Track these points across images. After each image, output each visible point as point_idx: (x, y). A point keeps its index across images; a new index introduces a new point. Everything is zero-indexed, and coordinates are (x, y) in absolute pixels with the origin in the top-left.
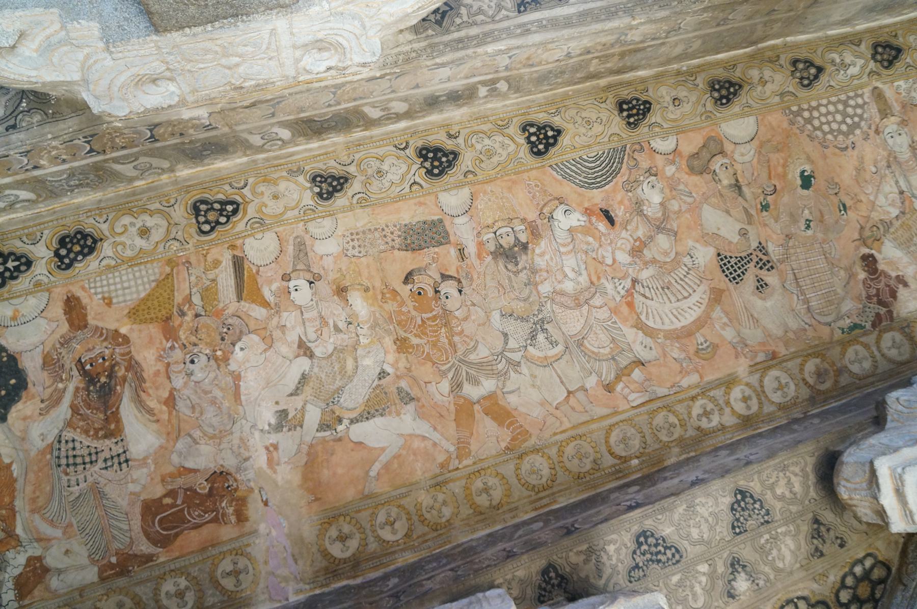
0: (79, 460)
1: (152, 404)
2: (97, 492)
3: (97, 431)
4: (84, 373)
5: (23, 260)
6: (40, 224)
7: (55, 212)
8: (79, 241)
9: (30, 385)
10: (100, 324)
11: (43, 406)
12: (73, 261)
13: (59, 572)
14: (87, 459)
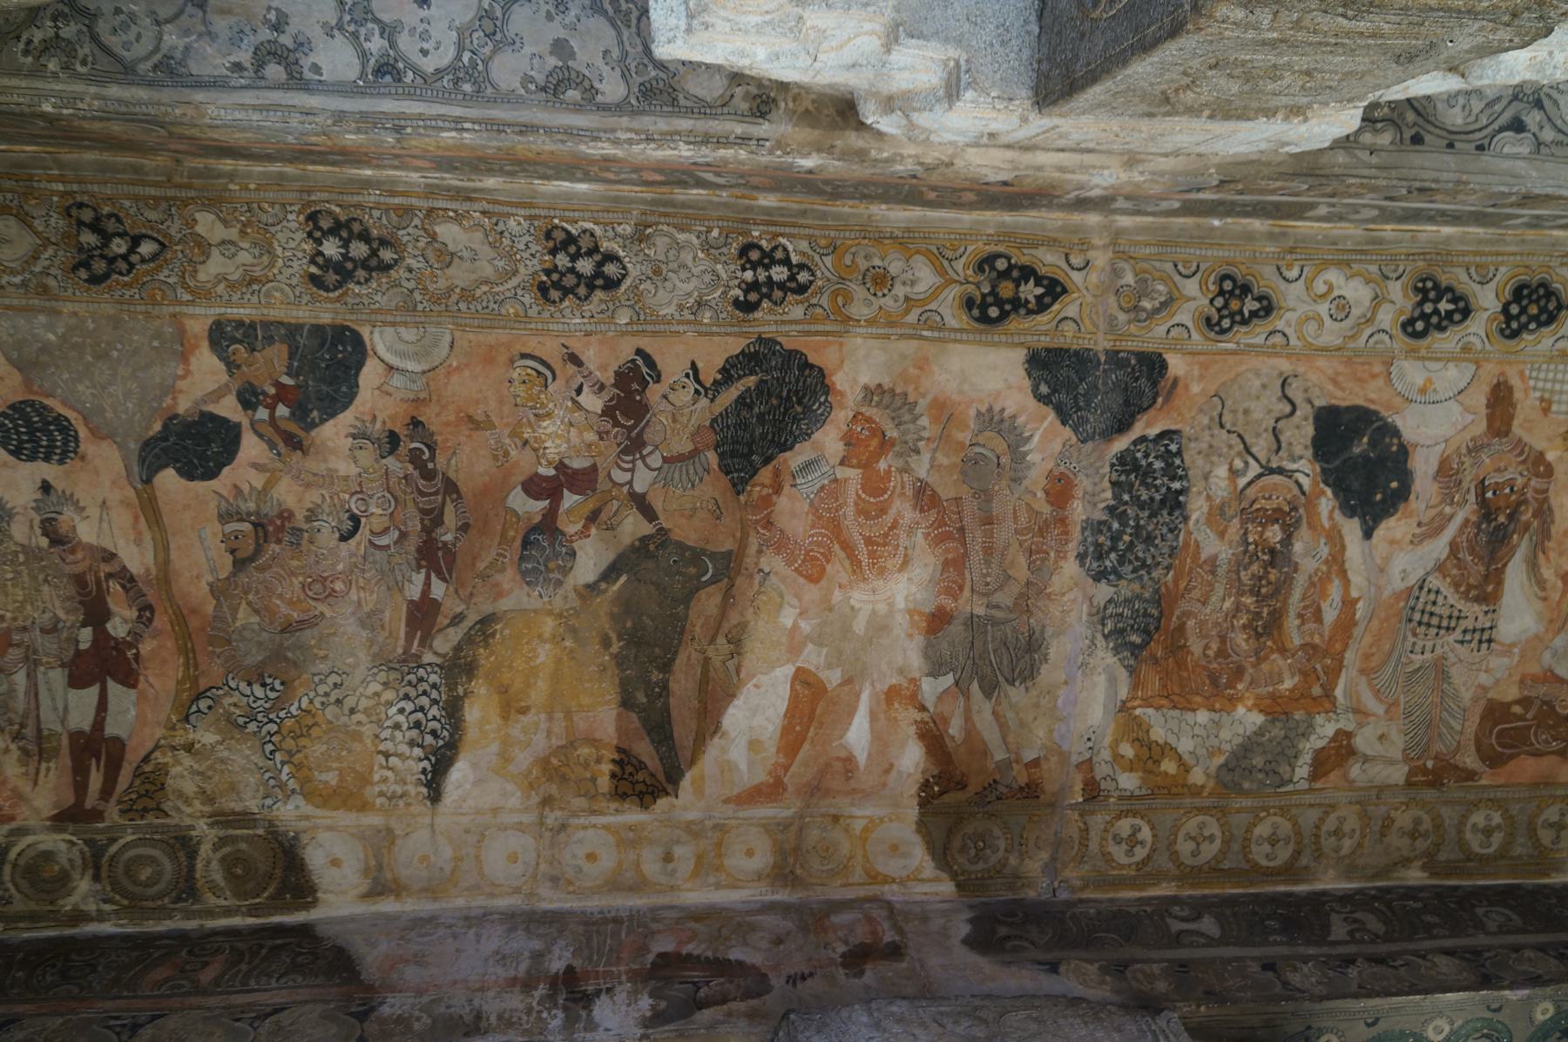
0: (1435, 621)
1: (1547, 573)
2: (1440, 670)
3: (1470, 587)
4: (1482, 502)
5: (1461, 304)
6: (1498, 254)
7: (1523, 241)
8: (1539, 298)
9: (1412, 497)
10: (1526, 438)
11: (1418, 531)
12: (1523, 328)
13: (1366, 759)
14: (1445, 623)
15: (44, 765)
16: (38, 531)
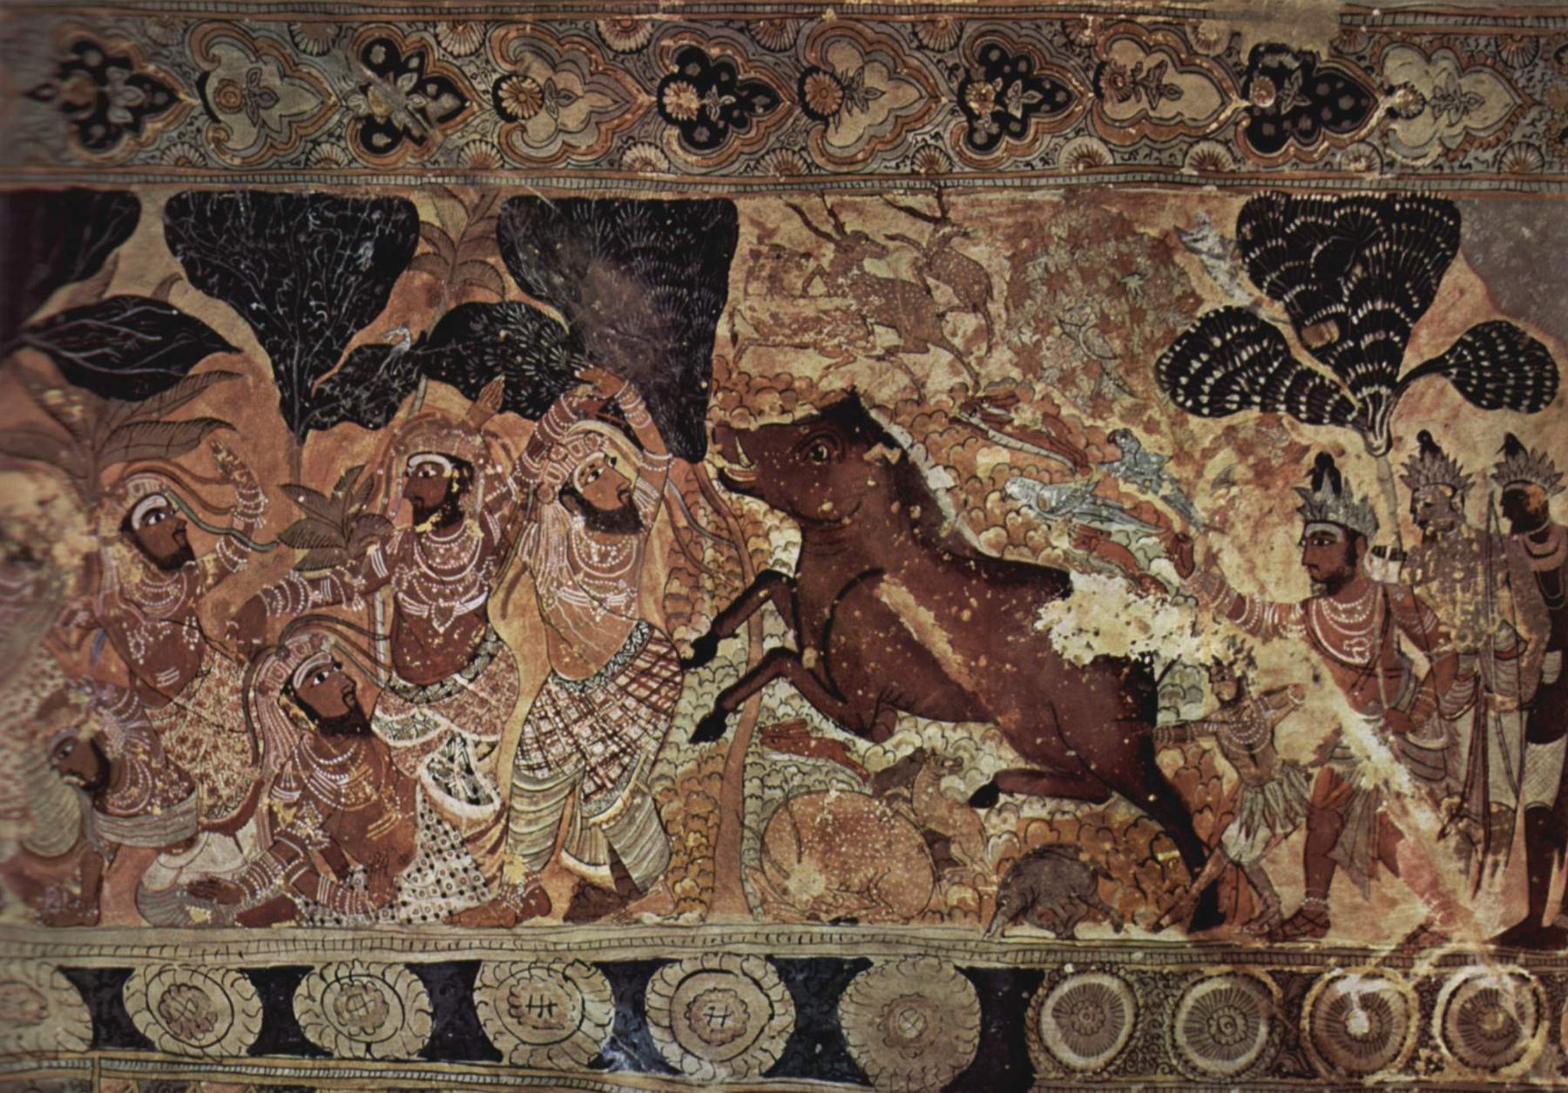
15: (1490, 859)
16: (1499, 510)
